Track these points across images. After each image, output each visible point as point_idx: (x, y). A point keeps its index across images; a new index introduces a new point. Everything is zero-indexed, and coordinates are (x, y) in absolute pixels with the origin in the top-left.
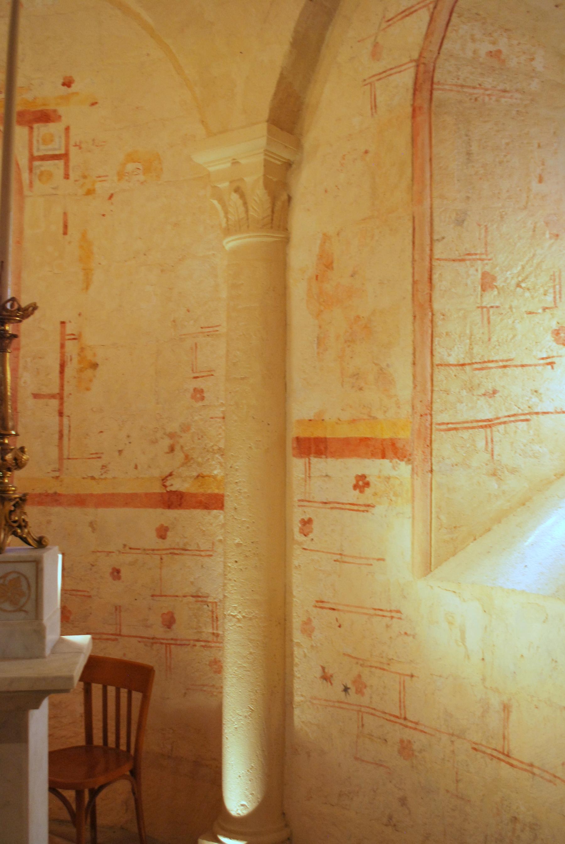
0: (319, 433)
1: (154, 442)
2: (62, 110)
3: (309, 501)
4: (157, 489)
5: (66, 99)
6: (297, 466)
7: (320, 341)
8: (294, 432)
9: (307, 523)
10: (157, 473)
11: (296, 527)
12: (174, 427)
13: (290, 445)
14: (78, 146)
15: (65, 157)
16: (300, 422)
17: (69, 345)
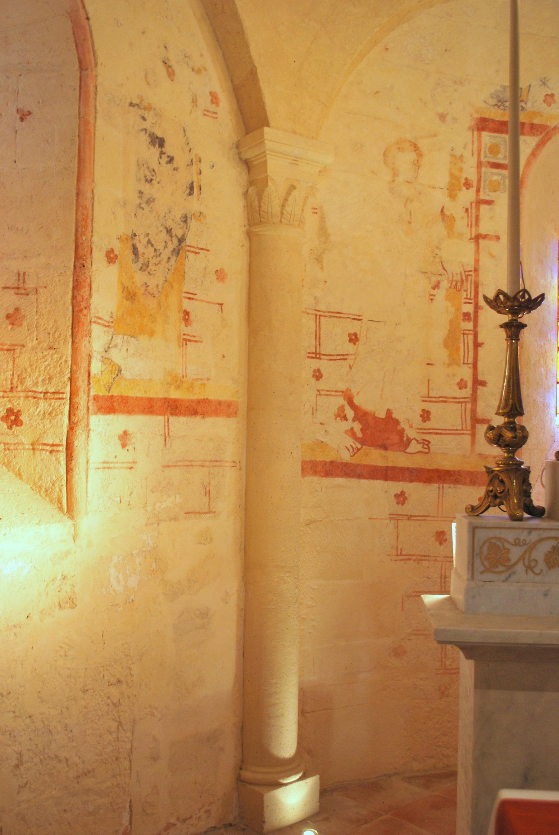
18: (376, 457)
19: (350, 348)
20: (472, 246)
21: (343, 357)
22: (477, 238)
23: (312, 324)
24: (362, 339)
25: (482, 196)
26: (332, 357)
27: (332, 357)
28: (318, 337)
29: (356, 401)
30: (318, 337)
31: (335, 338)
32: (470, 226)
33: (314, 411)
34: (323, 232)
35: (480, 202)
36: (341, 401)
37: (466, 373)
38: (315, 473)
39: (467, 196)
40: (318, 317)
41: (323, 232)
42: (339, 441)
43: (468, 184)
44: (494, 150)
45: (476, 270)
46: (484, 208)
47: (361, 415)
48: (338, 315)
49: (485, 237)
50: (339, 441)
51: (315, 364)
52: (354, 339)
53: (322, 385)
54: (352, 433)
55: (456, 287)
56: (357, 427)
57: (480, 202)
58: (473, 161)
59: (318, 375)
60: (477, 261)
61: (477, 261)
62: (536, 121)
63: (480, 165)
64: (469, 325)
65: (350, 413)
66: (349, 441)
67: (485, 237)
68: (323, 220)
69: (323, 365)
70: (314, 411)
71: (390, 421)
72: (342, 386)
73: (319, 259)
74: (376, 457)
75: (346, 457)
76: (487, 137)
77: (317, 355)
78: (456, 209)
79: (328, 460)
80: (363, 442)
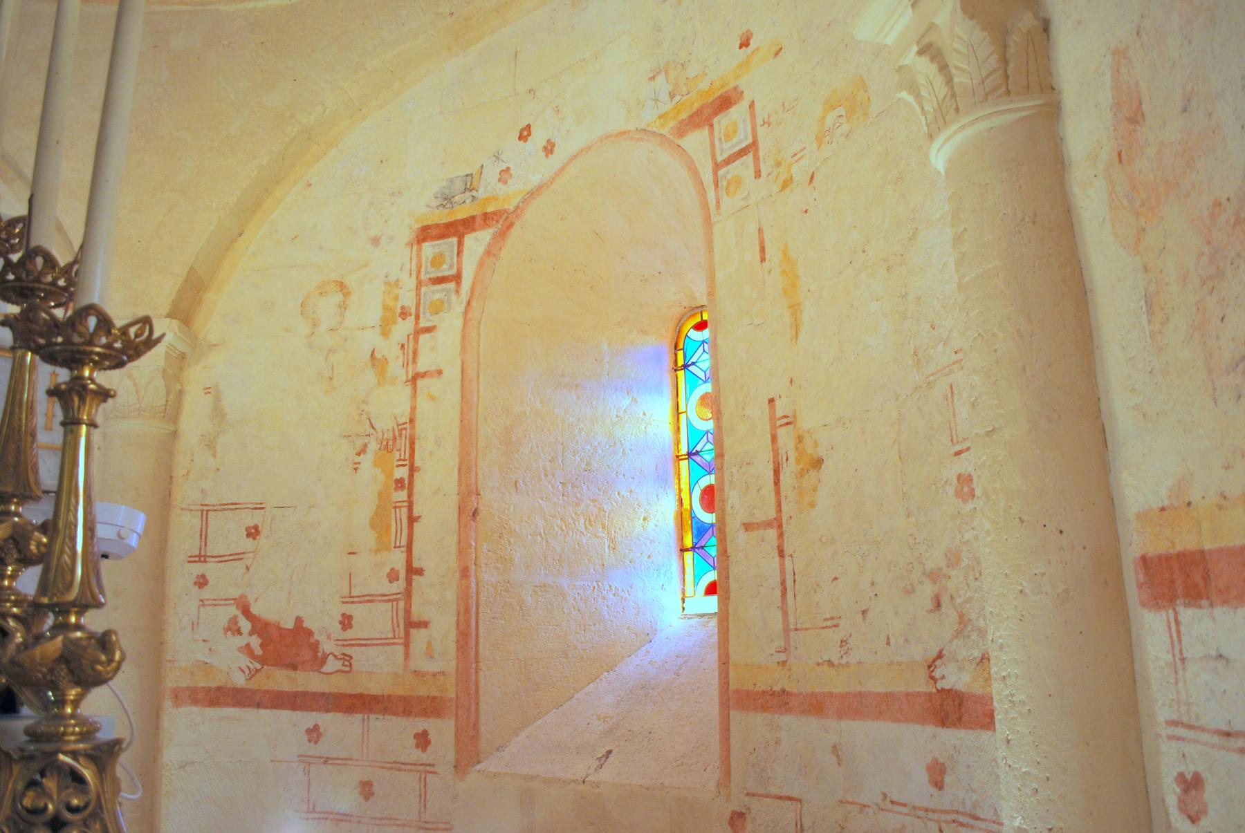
0: (1185, 541)
1: (910, 591)
2: (743, 83)
3: (1190, 727)
4: (922, 686)
5: (745, 64)
6: (1152, 626)
7: (1150, 303)
8: (1137, 543)
9: (1191, 784)
10: (918, 652)
11: (1171, 795)
12: (935, 559)
13: (1131, 576)
14: (766, 123)
15: (753, 147)
16: (1143, 516)
17: (782, 433)
18: (281, 680)
19: (249, 544)
20: (408, 390)
21: (238, 557)
22: (414, 379)
23: (196, 522)
24: (264, 531)
25: (423, 324)
26: (221, 559)
27: (221, 559)
28: (204, 537)
29: (255, 610)
30: (204, 537)
31: (227, 533)
32: (405, 365)
33: (194, 626)
34: (218, 413)
35: (419, 332)
36: (233, 611)
37: (397, 560)
38: (195, 702)
39: (404, 328)
40: (205, 512)
41: (218, 413)
42: (231, 661)
43: (404, 314)
44: (437, 261)
45: (412, 421)
46: (424, 338)
47: (261, 627)
48: (234, 506)
49: (423, 375)
50: (231, 661)
51: (198, 569)
52: (253, 532)
53: (207, 593)
54: (248, 650)
55: (387, 447)
56: (255, 642)
57: (419, 332)
58: (412, 283)
59: (202, 582)
60: (413, 408)
61: (413, 408)
62: (490, 209)
63: (419, 284)
64: (403, 495)
65: (245, 625)
66: (245, 661)
67: (423, 375)
68: (218, 399)
69: (210, 569)
70: (194, 626)
71: (300, 632)
72: (235, 592)
73: (211, 445)
74: (281, 680)
75: (240, 680)
76: (429, 249)
77: (201, 558)
78: (390, 350)
79: (214, 685)
80: (263, 661)
